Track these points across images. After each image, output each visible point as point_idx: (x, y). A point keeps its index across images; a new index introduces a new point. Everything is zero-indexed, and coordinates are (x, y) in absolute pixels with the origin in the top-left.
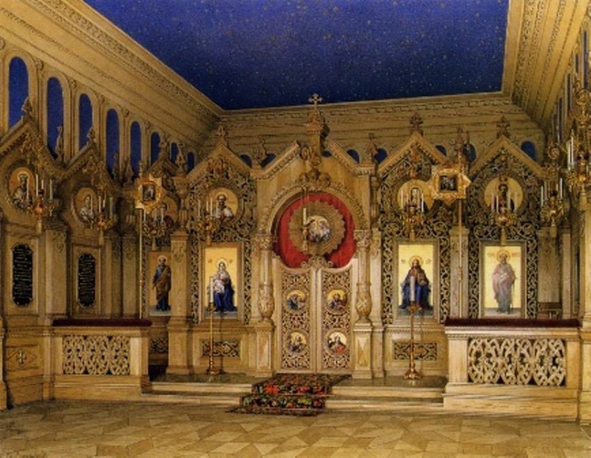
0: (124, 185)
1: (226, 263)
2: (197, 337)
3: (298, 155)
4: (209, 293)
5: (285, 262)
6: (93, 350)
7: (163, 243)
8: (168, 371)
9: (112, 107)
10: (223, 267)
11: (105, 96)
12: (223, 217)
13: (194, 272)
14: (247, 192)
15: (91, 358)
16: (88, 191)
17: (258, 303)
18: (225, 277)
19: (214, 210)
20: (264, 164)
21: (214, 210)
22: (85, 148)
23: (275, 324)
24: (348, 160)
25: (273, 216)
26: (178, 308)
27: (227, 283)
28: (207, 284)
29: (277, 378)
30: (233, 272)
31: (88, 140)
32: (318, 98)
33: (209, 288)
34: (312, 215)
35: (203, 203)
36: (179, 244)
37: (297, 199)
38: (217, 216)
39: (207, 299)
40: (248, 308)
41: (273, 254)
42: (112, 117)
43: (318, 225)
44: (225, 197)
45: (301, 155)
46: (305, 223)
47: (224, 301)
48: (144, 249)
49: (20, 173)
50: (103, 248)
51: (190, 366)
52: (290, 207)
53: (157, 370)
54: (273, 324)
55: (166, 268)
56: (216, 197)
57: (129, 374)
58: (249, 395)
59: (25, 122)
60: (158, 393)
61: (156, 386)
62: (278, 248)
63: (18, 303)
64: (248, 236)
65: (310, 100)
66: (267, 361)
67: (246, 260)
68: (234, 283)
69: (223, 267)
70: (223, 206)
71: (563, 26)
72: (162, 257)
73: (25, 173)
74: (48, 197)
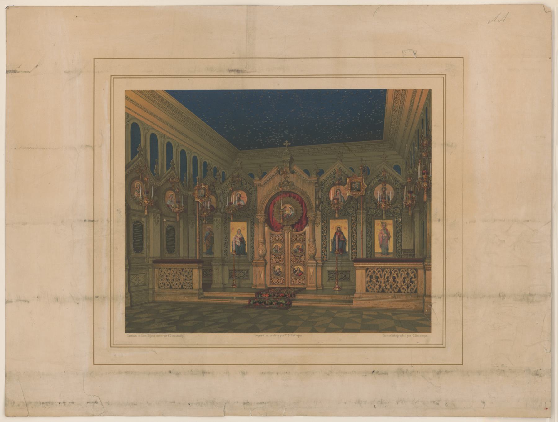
0: (189, 189)
1: (241, 229)
2: (226, 268)
3: (278, 173)
4: (233, 246)
5: (272, 228)
6: (186, 276)
7: (210, 220)
8: (213, 286)
9: (154, 132)
10: (239, 232)
11: (129, 113)
12: (240, 205)
13: (227, 233)
14: (252, 193)
15: (173, 280)
16: (172, 192)
17: (260, 249)
18: (241, 237)
19: (235, 202)
20: (261, 178)
21: (235, 202)
22: (169, 171)
23: (267, 261)
24: (304, 175)
25: (265, 205)
26: (217, 253)
27: (242, 240)
28: (231, 240)
29: (268, 289)
30: (245, 235)
31: (138, 152)
32: (288, 143)
33: (232, 242)
34: (285, 204)
35: (229, 199)
36: (218, 219)
37: (278, 195)
38: (237, 204)
39: (232, 249)
40: (253, 253)
41: (266, 224)
42: (154, 138)
43: (289, 211)
44: (241, 195)
45: (279, 173)
46: (281, 208)
47: (240, 250)
48: (199, 222)
49: (136, 183)
50: (179, 222)
51: (223, 284)
52: (272, 201)
53: (207, 286)
54: (265, 260)
55: (211, 232)
56: (236, 194)
57: (192, 288)
58: (253, 299)
59: (139, 157)
60: (207, 297)
61: (206, 294)
62: (269, 221)
63: (136, 251)
64: (253, 215)
65: (284, 144)
66: (263, 280)
67: (252, 228)
68: (246, 239)
69: (239, 232)
70: (239, 200)
71: (415, 105)
72: (209, 227)
73: (139, 183)
74: (151, 196)
